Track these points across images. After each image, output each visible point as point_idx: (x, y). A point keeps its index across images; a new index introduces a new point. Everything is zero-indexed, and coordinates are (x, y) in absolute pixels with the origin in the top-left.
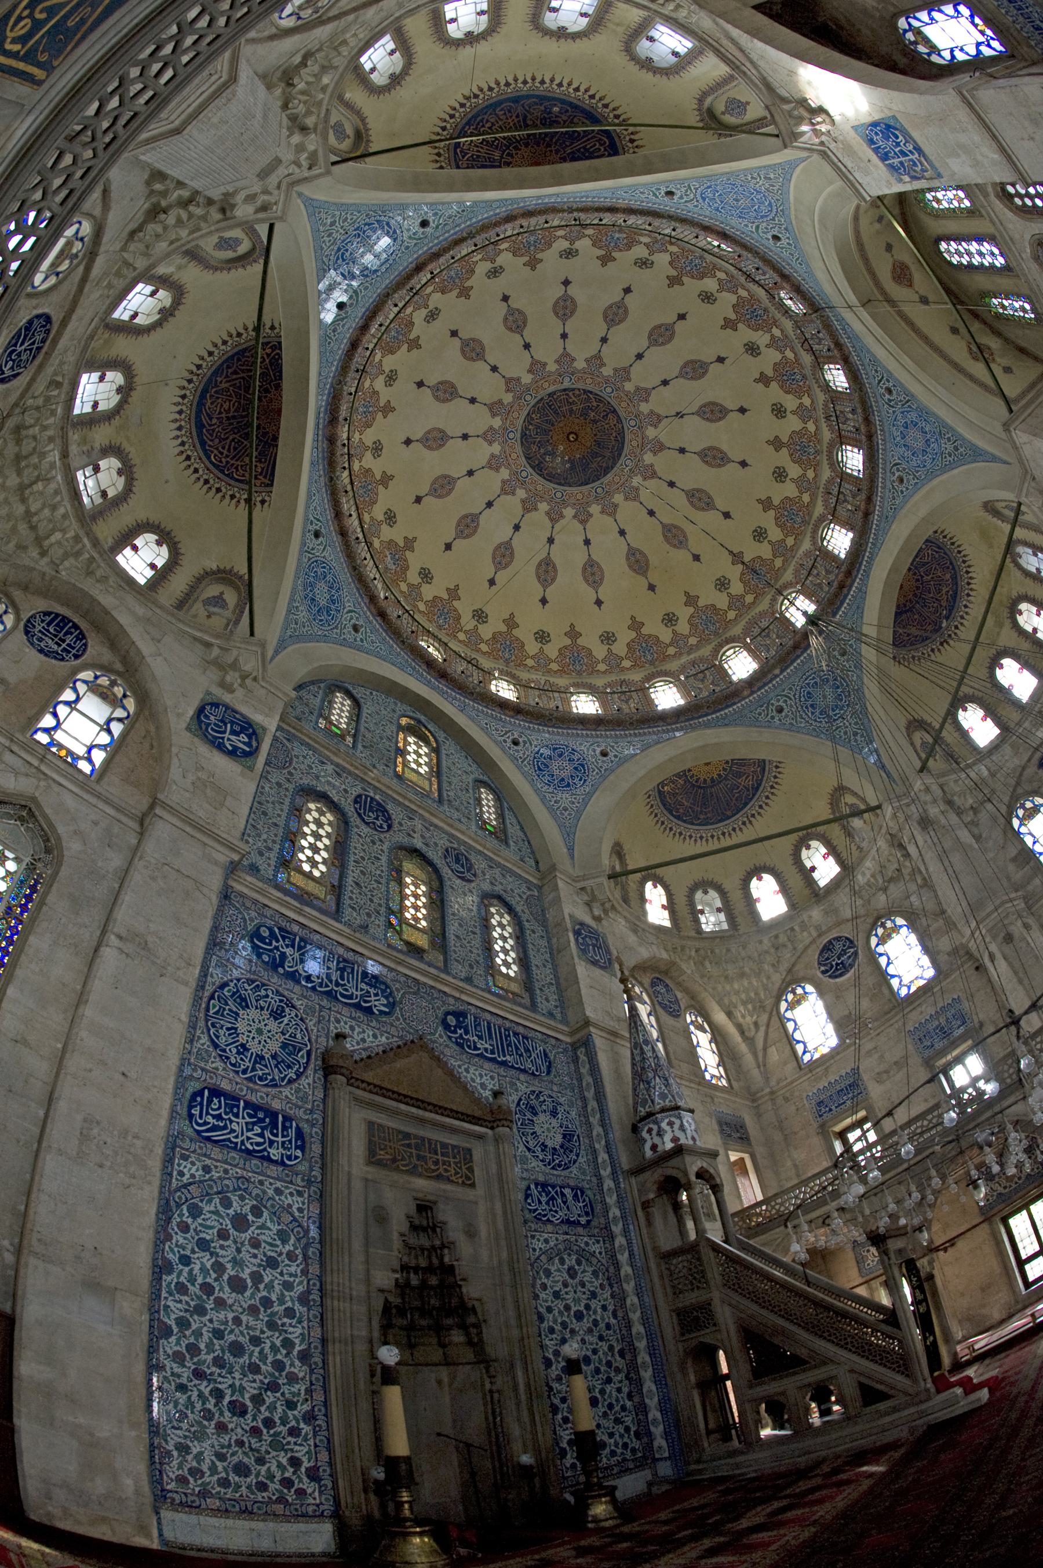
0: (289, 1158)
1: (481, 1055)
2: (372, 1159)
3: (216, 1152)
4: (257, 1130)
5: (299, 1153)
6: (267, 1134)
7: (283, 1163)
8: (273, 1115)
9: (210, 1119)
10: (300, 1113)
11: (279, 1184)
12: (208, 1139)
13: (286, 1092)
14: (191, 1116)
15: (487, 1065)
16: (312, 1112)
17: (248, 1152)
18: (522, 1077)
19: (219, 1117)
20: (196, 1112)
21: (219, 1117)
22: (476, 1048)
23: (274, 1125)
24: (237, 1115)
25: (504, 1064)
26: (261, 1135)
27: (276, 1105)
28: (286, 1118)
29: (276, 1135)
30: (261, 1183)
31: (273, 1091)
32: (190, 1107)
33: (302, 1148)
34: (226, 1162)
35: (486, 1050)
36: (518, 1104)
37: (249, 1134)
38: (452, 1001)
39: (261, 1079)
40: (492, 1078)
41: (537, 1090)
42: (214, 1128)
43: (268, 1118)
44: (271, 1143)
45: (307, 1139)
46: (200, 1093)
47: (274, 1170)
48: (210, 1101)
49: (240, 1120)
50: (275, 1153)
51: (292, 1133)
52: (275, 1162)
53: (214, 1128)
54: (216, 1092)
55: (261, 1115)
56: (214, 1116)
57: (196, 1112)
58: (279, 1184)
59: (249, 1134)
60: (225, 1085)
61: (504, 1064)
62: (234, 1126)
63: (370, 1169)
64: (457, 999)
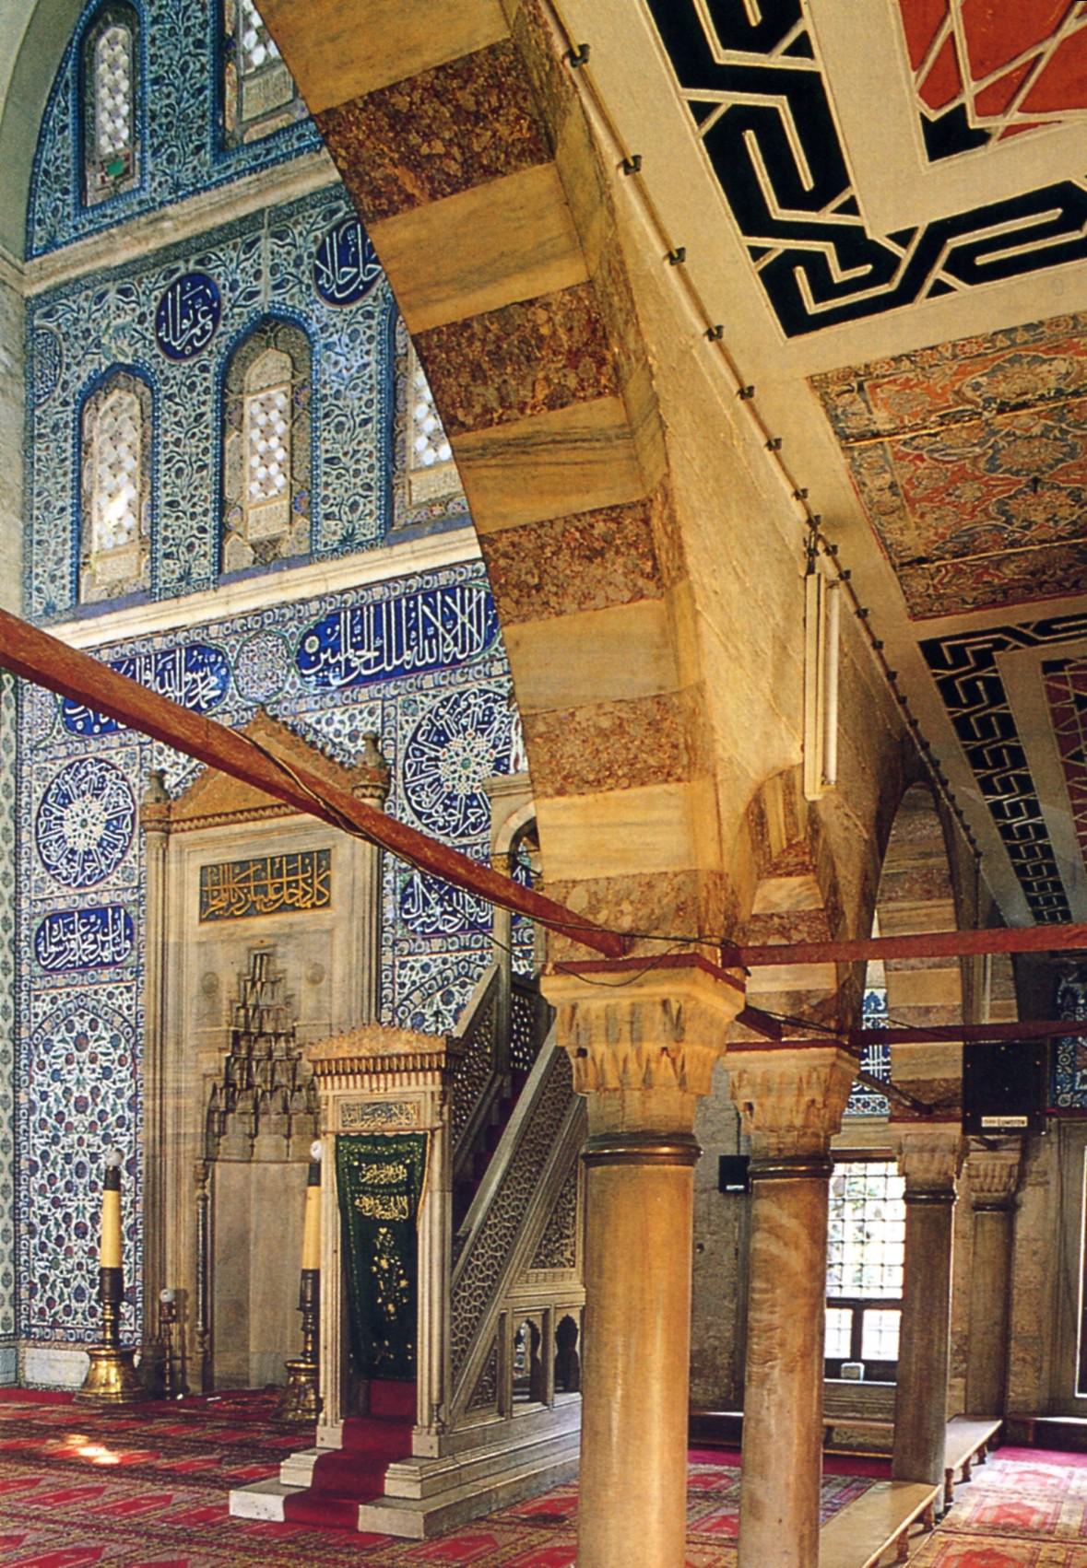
0: (119, 954)
1: (362, 681)
2: (208, 915)
3: (59, 980)
4: (91, 937)
5: (128, 944)
6: (99, 937)
7: (114, 963)
8: (101, 912)
9: (53, 949)
10: (128, 897)
11: (110, 988)
12: (53, 969)
13: (112, 879)
14: (38, 954)
15: (364, 693)
16: (138, 887)
17: (85, 965)
18: (428, 681)
19: (60, 943)
20: (41, 949)
21: (60, 943)
22: (350, 670)
23: (105, 924)
24: (73, 932)
25: (399, 672)
26: (95, 942)
27: (105, 900)
28: (116, 909)
29: (105, 935)
30: (96, 993)
31: (101, 886)
32: (37, 945)
33: (129, 938)
34: (68, 985)
35: (367, 665)
36: (414, 739)
37: (85, 946)
38: (315, 605)
39: (90, 878)
40: (371, 713)
41: (452, 691)
42: (59, 954)
43: (98, 917)
44: (103, 943)
45: (135, 922)
46: (42, 927)
47: (107, 974)
48: (51, 928)
49: (77, 935)
50: (107, 955)
51: (121, 924)
52: (108, 964)
53: (59, 954)
54: (54, 917)
55: (93, 919)
56: (56, 944)
57: (41, 949)
58: (110, 988)
59: (85, 946)
60: (61, 905)
61: (399, 672)
62: (73, 945)
63: (207, 926)
64: (320, 598)
